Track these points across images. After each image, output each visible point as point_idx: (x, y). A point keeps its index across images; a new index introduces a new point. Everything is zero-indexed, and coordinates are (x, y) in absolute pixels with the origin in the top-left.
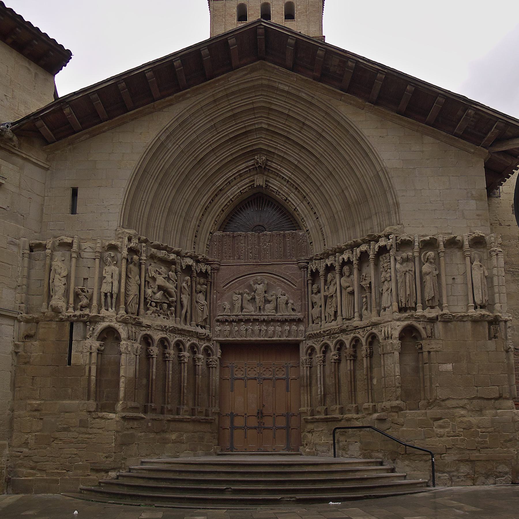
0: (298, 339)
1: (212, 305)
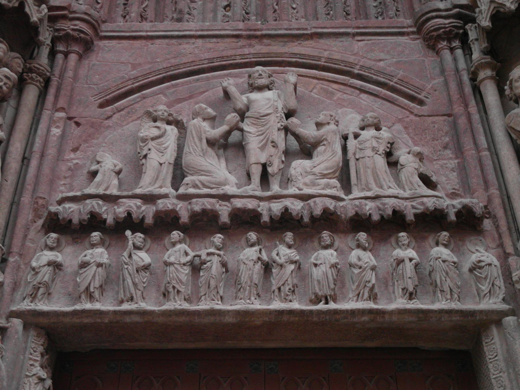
0: (469, 306)
1: (34, 163)
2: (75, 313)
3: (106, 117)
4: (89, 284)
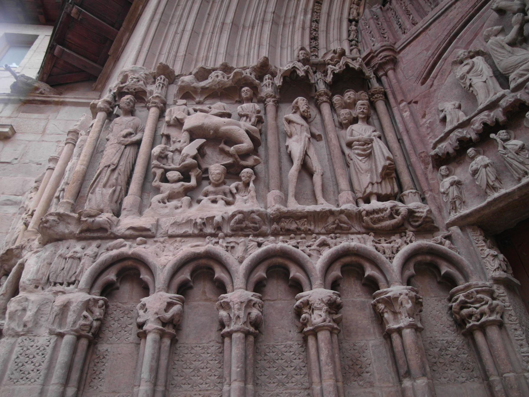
1: (405, 138)
2: (490, 204)
3: (429, 87)
4: (487, 181)
